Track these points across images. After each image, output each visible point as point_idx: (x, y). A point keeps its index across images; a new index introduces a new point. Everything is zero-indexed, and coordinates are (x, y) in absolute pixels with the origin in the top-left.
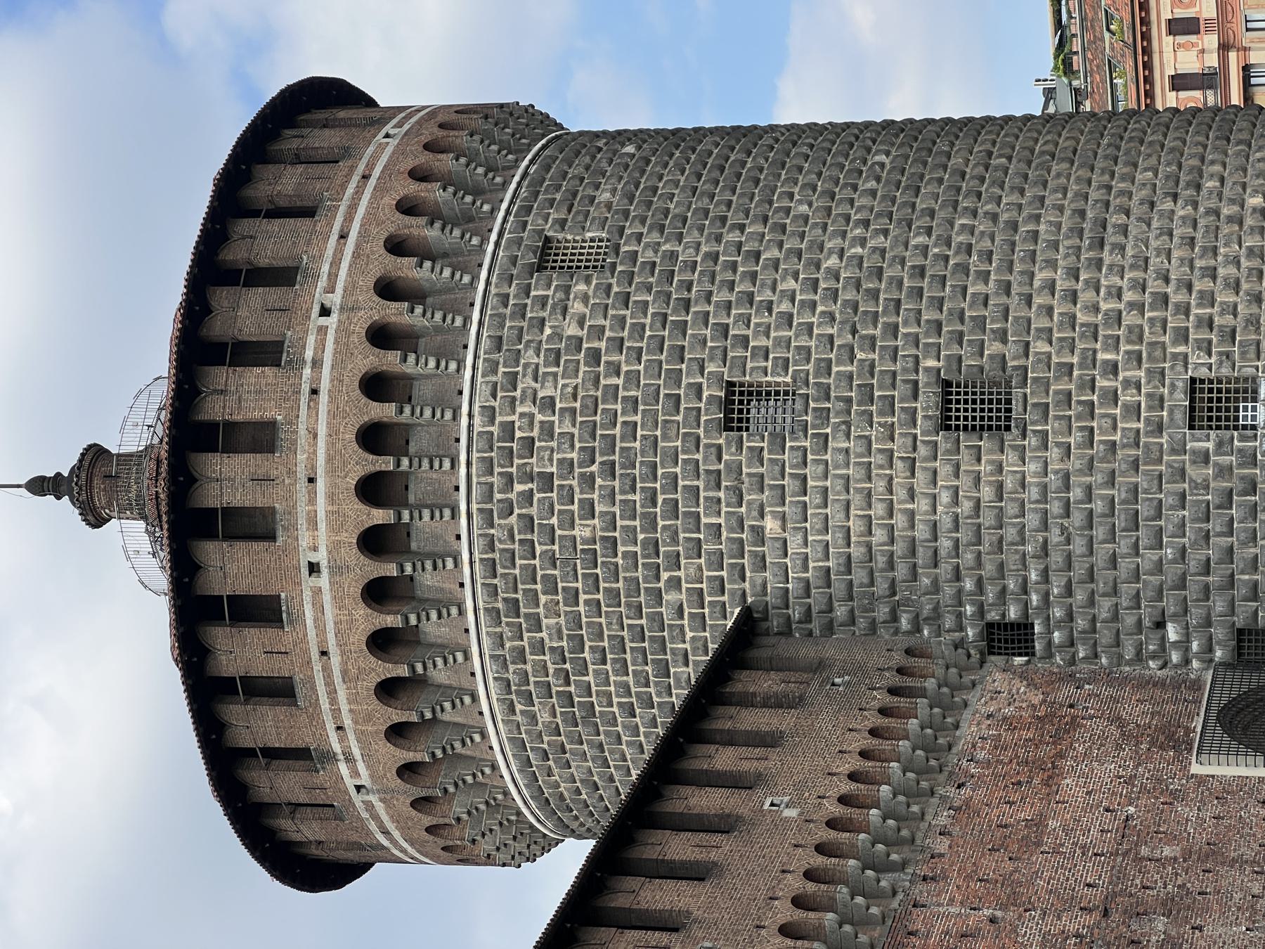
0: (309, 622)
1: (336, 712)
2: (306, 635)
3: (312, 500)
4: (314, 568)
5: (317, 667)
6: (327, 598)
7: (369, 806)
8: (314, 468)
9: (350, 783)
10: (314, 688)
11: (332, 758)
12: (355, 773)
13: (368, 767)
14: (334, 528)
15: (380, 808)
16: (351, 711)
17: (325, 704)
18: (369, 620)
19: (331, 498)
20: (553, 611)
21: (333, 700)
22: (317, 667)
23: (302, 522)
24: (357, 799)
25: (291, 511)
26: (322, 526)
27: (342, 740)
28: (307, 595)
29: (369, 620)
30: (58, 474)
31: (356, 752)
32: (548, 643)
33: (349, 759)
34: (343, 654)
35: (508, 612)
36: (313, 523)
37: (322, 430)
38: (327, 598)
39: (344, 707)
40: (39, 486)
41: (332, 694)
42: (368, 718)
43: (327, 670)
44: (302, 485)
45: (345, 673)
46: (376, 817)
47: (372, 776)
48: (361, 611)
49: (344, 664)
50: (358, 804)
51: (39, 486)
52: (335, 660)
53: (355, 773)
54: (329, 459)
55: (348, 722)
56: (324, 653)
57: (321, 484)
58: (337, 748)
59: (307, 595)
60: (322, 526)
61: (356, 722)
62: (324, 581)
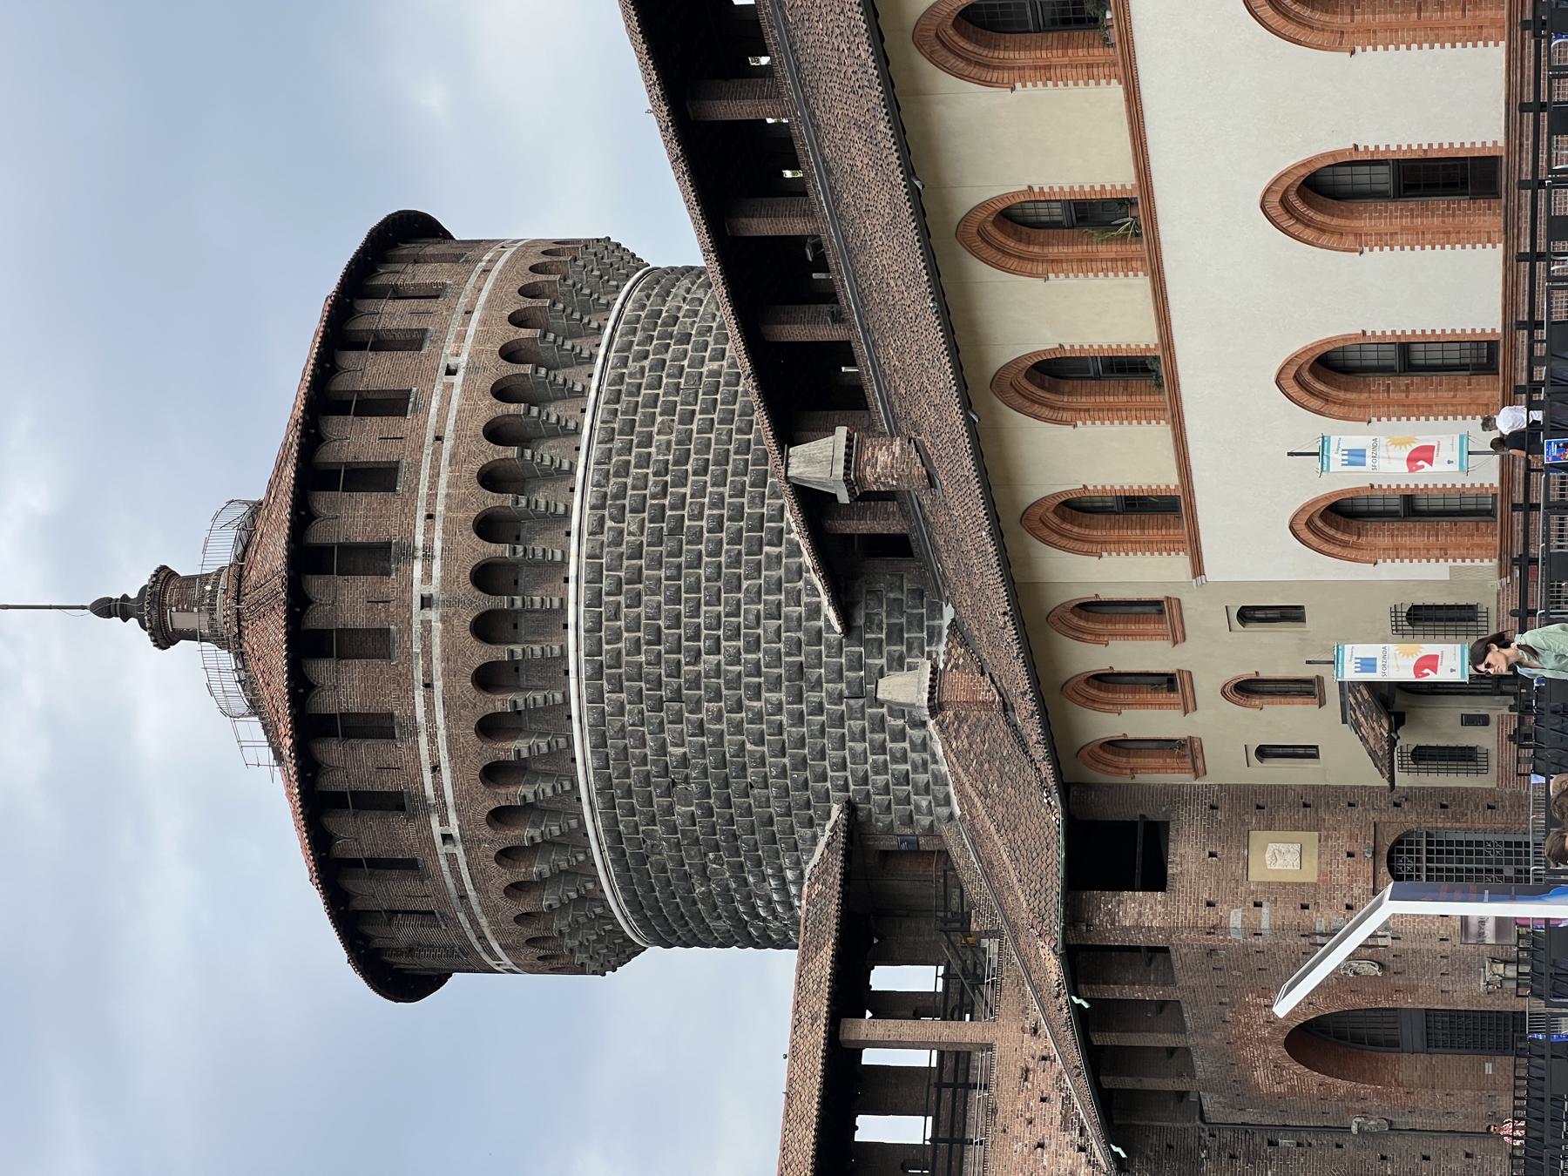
0: (433, 410)
1: (432, 497)
2: (426, 422)
3: (465, 324)
4: (451, 372)
5: (428, 451)
6: (457, 391)
7: (427, 625)
8: (473, 306)
9: (418, 589)
10: (418, 473)
11: (408, 553)
12: (428, 577)
13: (444, 566)
14: (478, 339)
15: (437, 626)
16: (447, 495)
17: (423, 489)
18: (491, 409)
19: (483, 322)
20: (666, 429)
21: (433, 485)
22: (428, 451)
23: (451, 337)
24: (418, 615)
25: (443, 331)
26: (469, 340)
27: (429, 530)
28: (438, 388)
29: (491, 409)
30: (125, 598)
31: (438, 545)
32: (654, 457)
33: (428, 557)
34: (458, 437)
35: (625, 428)
36: (461, 337)
37: (488, 287)
38: (457, 391)
39: (442, 490)
40: (105, 608)
41: (433, 485)
42: (463, 504)
43: (437, 454)
44: (458, 316)
45: (453, 456)
46: (427, 652)
47: (443, 579)
48: (490, 400)
49: (456, 446)
50: (417, 627)
51: (105, 608)
52: (448, 445)
53: (428, 577)
54: (489, 301)
55: (440, 508)
56: (438, 438)
57: (476, 316)
58: (419, 540)
59: (438, 388)
60: (469, 340)
61: (448, 508)
62: (458, 379)
